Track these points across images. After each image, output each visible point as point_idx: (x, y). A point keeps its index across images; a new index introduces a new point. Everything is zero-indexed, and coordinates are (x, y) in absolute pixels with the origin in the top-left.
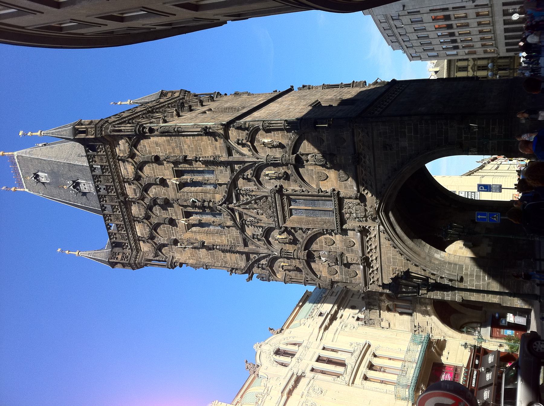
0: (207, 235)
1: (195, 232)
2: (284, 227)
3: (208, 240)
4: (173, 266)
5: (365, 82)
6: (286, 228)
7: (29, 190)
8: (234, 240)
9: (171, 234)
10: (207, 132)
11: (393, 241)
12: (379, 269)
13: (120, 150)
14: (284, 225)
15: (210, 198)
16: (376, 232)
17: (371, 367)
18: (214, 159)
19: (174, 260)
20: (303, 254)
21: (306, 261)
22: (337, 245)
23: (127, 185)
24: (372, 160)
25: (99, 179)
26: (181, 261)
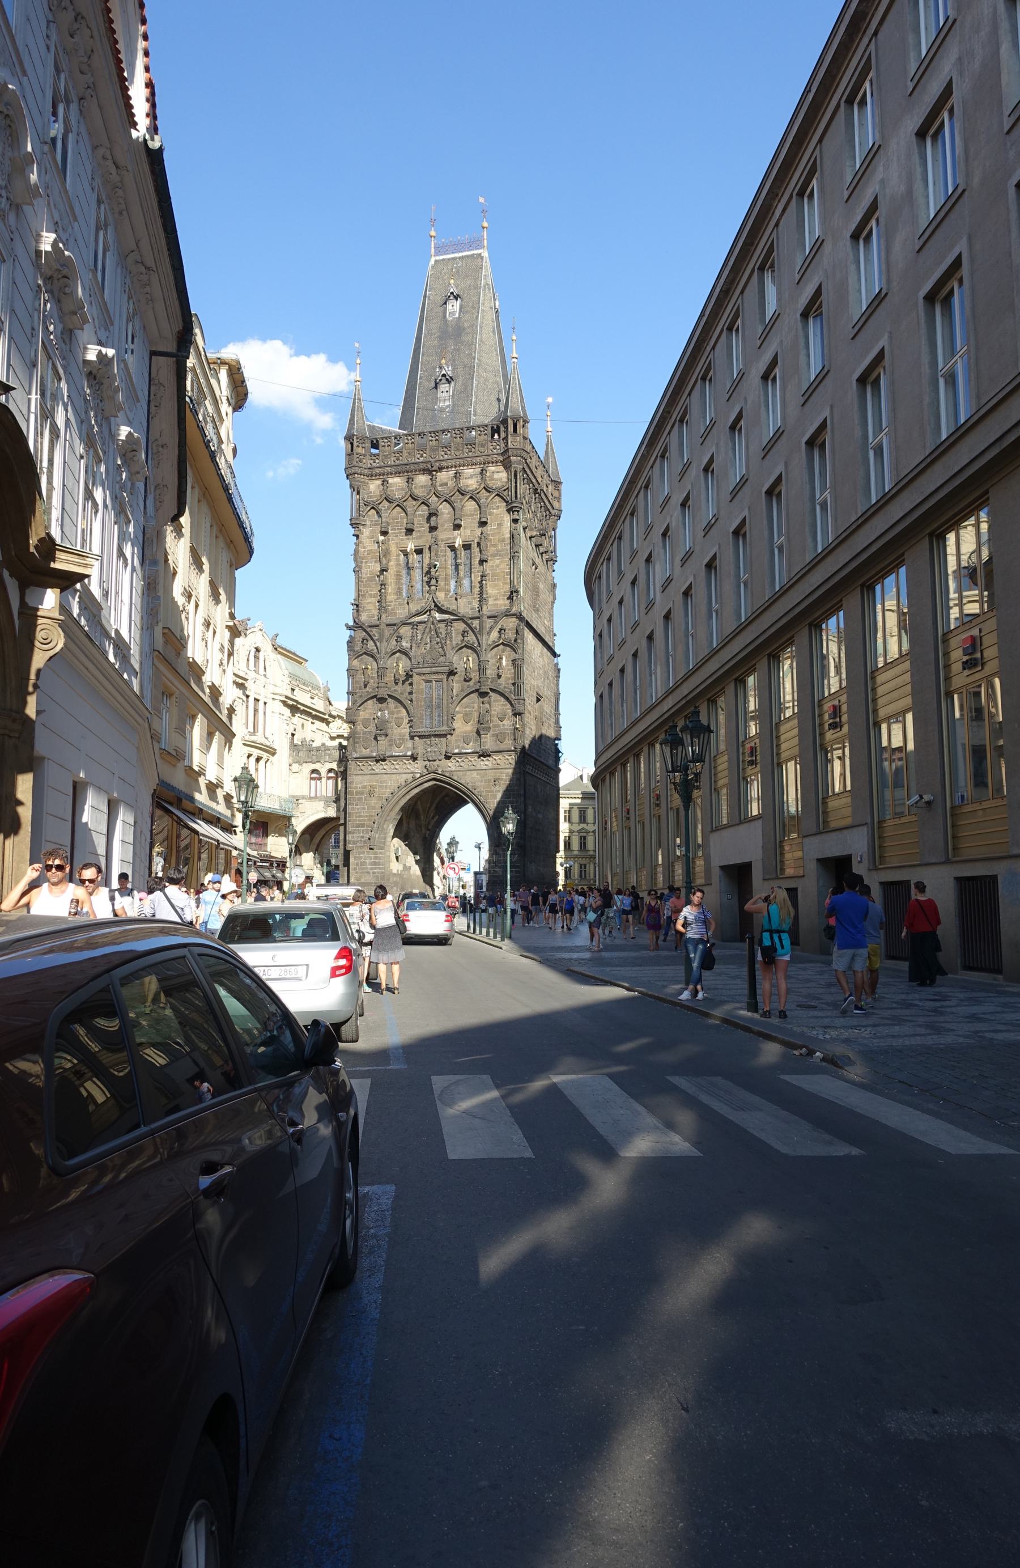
1: (398, 560)
3: (390, 577)
4: (354, 524)
5: (560, 739)
6: (411, 676)
7: (433, 267)
8: (392, 610)
12: (373, 772)
14: (414, 675)
17: (258, 760)
19: (361, 527)
20: (383, 693)
21: (375, 696)
23: (452, 473)
24: (485, 767)
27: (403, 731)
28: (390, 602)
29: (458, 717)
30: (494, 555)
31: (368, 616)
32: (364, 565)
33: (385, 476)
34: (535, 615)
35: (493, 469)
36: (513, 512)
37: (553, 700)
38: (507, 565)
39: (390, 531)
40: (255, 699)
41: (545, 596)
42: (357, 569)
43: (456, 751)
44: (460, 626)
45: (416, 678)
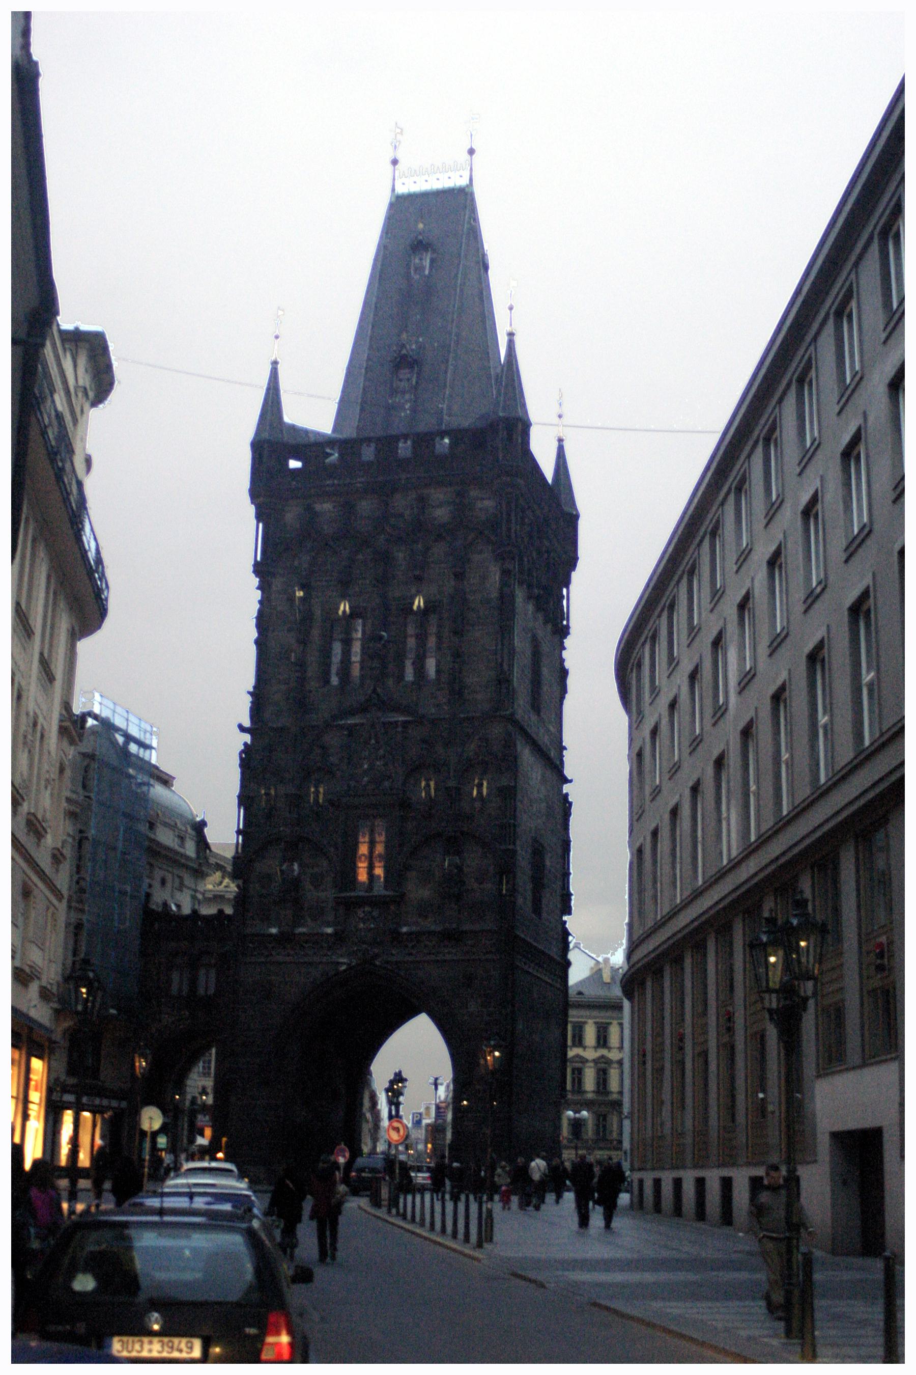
5: (570, 913)
10: (503, 681)
24: (448, 957)
27: (322, 895)
34: (534, 718)
35: (474, 493)
36: (504, 559)
37: (560, 851)
39: (313, 584)
41: (548, 689)
43: (405, 929)
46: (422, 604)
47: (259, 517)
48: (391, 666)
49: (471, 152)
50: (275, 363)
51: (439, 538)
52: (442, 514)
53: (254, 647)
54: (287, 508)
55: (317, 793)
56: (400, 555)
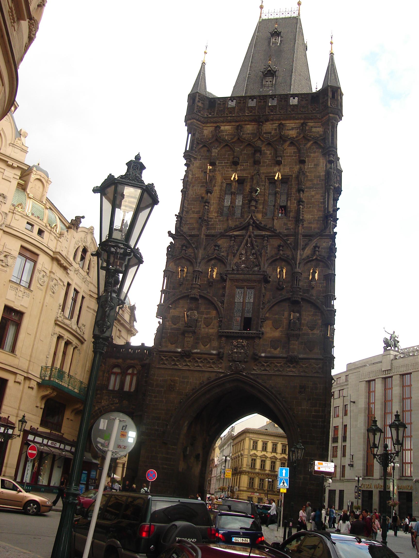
0: (218, 198)
2: (227, 279)
3: (213, 198)
6: (225, 281)
8: (212, 225)
9: (221, 161)
11: (207, 384)
12: (176, 367)
13: (311, 127)
15: (258, 208)
16: (216, 369)
18: (301, 220)
19: (192, 159)
20: (195, 293)
22: (203, 330)
24: (291, 374)
25: (283, 100)
26: (191, 165)
27: (211, 331)
28: (212, 218)
29: (269, 323)
30: (310, 188)
31: (189, 229)
32: (191, 188)
33: (218, 124)
35: (311, 124)
38: (321, 196)
39: (217, 164)
40: (75, 290)
42: (185, 190)
43: (263, 355)
44: (276, 242)
45: (228, 284)
46: (280, 177)
47: (189, 131)
48: (261, 207)
49: (299, 4)
50: (203, 64)
51: (292, 144)
52: (293, 133)
53: (181, 193)
54: (204, 128)
55: (212, 271)
56: (268, 152)
